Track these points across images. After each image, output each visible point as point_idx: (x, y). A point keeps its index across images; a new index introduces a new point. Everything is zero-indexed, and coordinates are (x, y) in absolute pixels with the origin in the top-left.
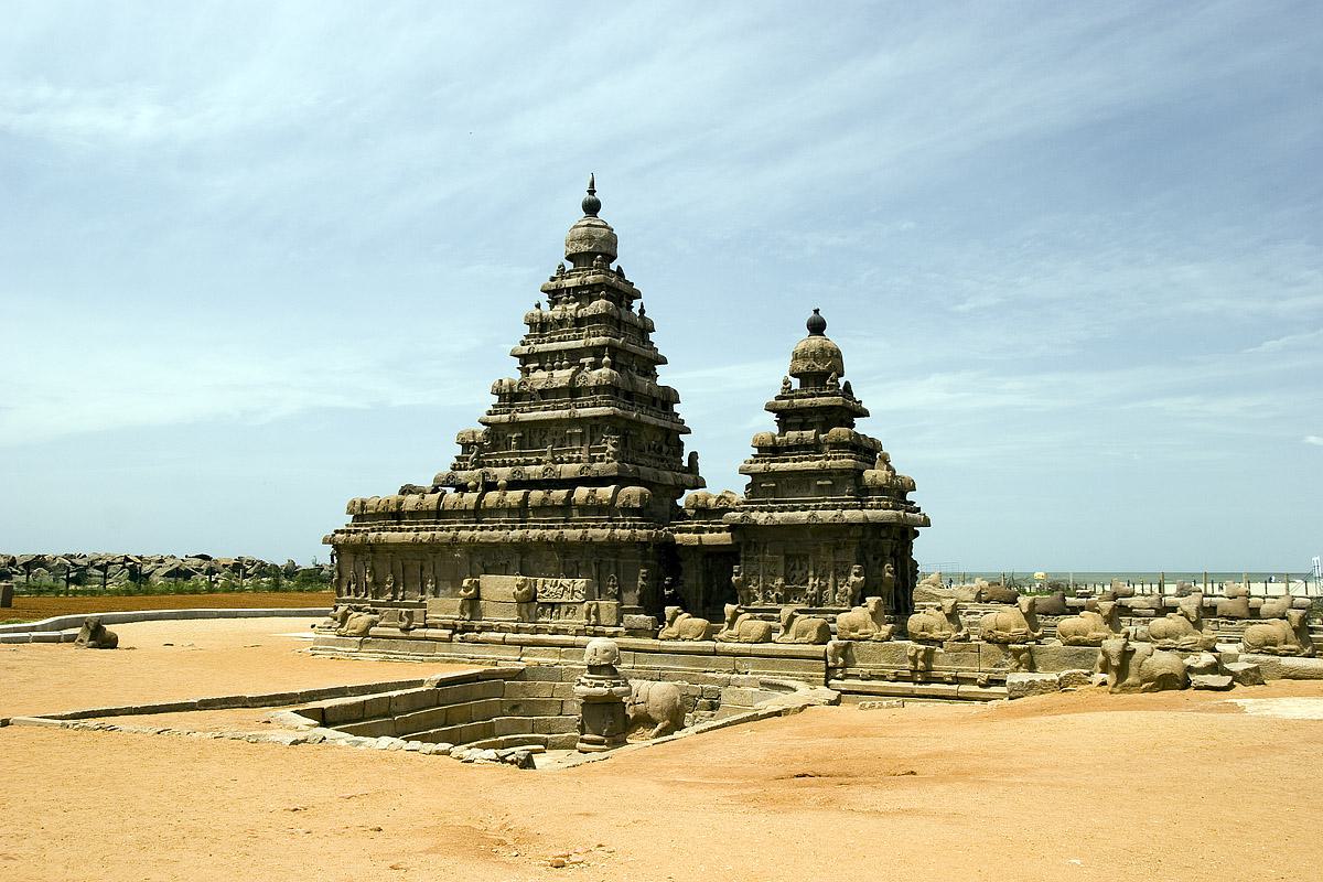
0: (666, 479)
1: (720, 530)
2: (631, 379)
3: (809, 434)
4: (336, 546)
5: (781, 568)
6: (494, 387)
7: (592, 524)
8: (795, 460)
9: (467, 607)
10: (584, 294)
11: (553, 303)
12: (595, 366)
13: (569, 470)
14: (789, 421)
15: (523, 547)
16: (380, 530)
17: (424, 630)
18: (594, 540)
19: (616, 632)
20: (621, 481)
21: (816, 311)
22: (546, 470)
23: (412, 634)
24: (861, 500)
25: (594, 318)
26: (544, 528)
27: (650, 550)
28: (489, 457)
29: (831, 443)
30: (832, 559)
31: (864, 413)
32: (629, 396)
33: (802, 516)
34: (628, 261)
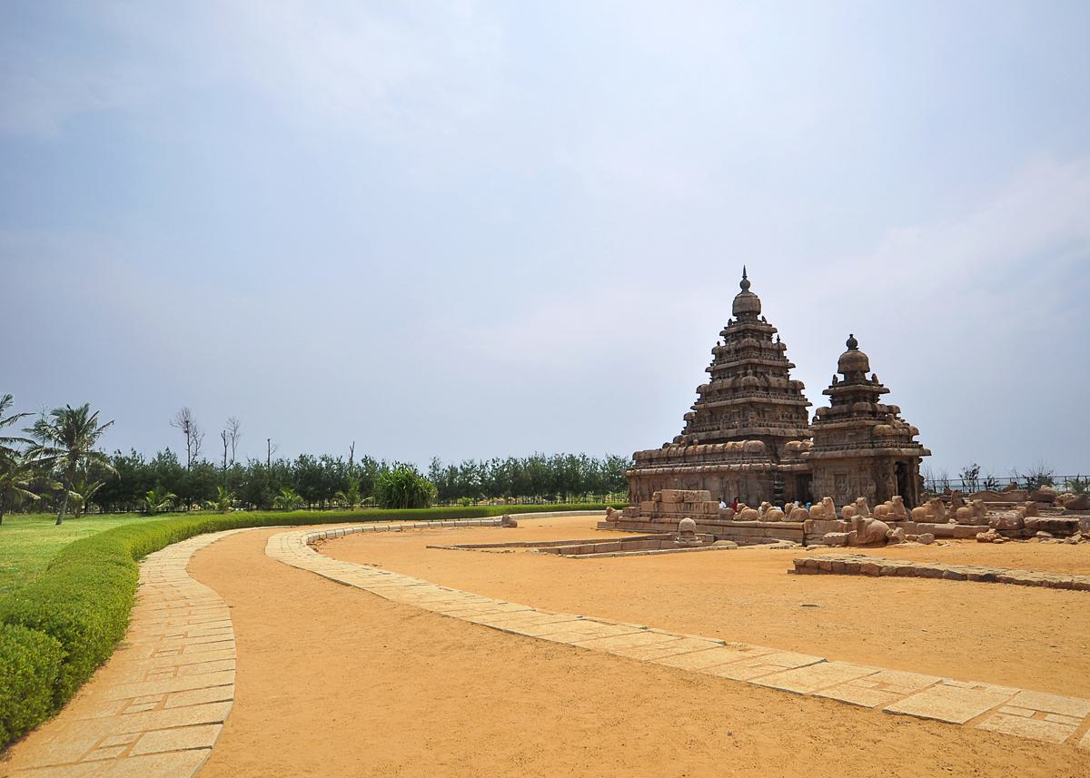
1: (802, 462)
2: (767, 380)
3: (844, 408)
5: (833, 482)
10: (742, 333)
12: (746, 375)
13: (732, 432)
14: (836, 400)
20: (748, 438)
21: (851, 335)
23: (634, 519)
25: (743, 349)
27: (763, 474)
32: (766, 389)
34: (769, 313)
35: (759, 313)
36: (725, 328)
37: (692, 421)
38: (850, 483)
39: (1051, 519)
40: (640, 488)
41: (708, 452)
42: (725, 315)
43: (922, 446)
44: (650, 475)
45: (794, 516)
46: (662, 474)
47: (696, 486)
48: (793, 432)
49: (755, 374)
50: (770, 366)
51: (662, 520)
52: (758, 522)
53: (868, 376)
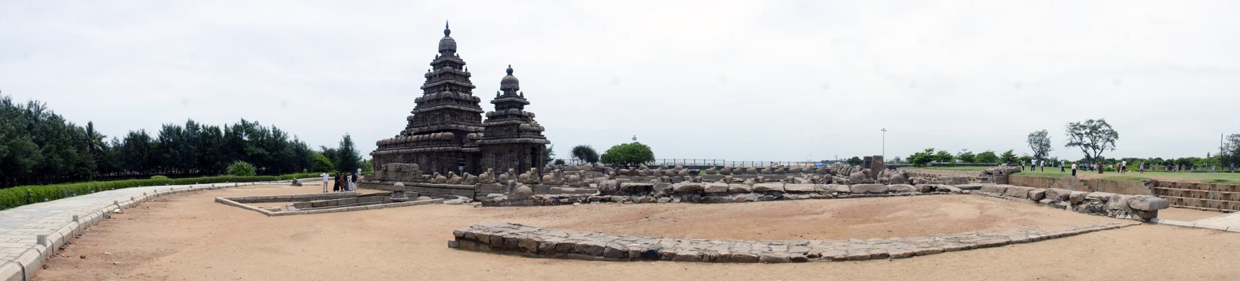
0: (471, 129)
1: (476, 147)
2: (458, 95)
3: (503, 112)
11: (434, 69)
12: (445, 90)
13: (435, 128)
15: (417, 154)
20: (445, 131)
25: (445, 73)
31: (528, 103)
34: (461, 52)
35: (455, 52)
37: (412, 121)
39: (637, 184)
42: (434, 52)
43: (545, 138)
44: (386, 155)
45: (468, 181)
47: (412, 161)
48: (473, 128)
49: (451, 90)
50: (461, 86)
52: (446, 184)
53: (518, 93)
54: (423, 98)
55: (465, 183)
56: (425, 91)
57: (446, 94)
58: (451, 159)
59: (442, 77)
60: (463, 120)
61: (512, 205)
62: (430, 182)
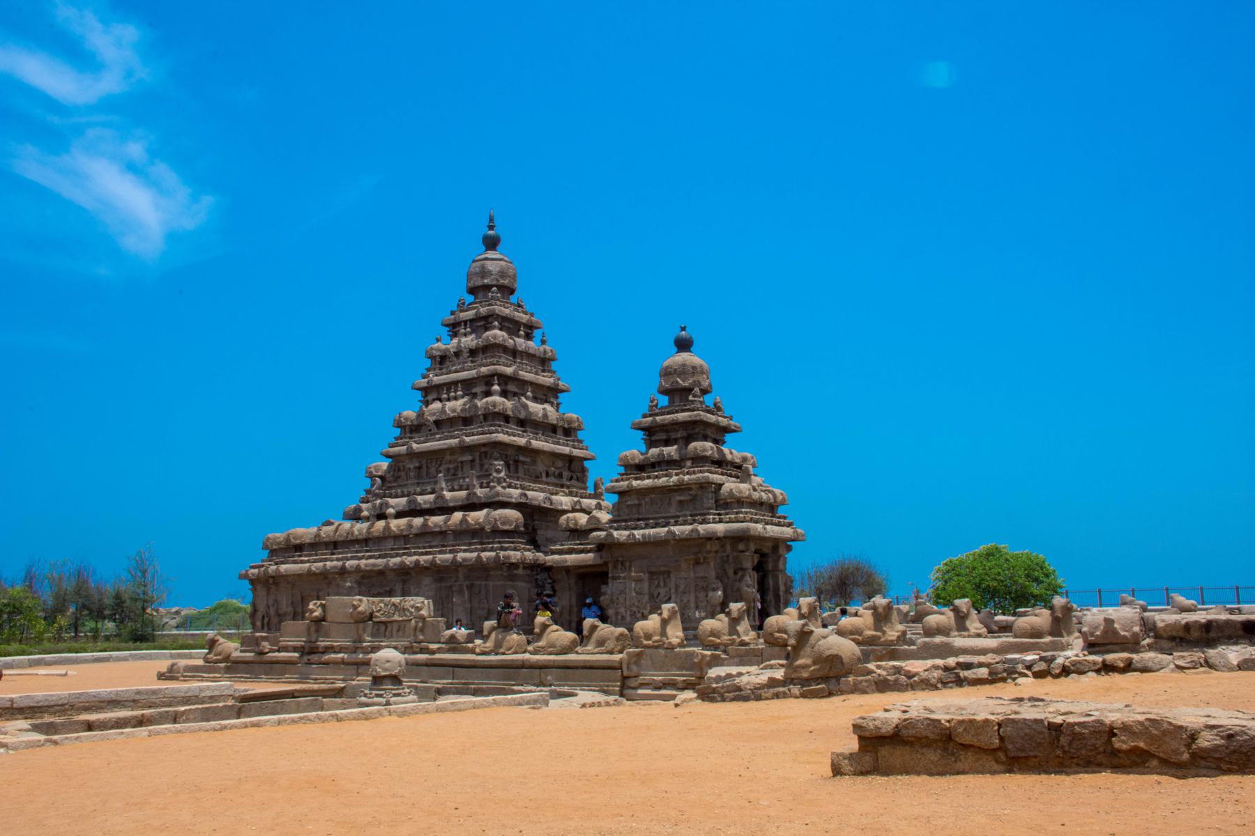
0: (561, 504)
1: (589, 551)
2: (525, 407)
3: (671, 451)
4: (252, 582)
5: (646, 585)
6: (395, 420)
7: (463, 548)
8: (657, 477)
9: (313, 629)
10: (482, 323)
12: (488, 393)
14: (653, 438)
16: (283, 563)
17: (276, 654)
18: (465, 563)
19: (439, 648)
22: (438, 497)
24: (719, 514)
26: (422, 554)
28: (391, 488)
29: (692, 459)
30: (692, 574)
32: (522, 423)
33: (662, 531)
35: (512, 291)
36: (453, 313)
38: (677, 587)
40: (276, 601)
41: (414, 531)
44: (299, 576)
45: (601, 643)
46: (321, 574)
49: (504, 394)
50: (531, 383)
51: (326, 657)
52: (527, 656)
53: (709, 400)
54: (420, 414)
55: (589, 648)
56: (426, 395)
57: (494, 405)
58: (514, 587)
59: (480, 359)
60: (536, 478)
61: (803, 695)
62: (472, 651)
